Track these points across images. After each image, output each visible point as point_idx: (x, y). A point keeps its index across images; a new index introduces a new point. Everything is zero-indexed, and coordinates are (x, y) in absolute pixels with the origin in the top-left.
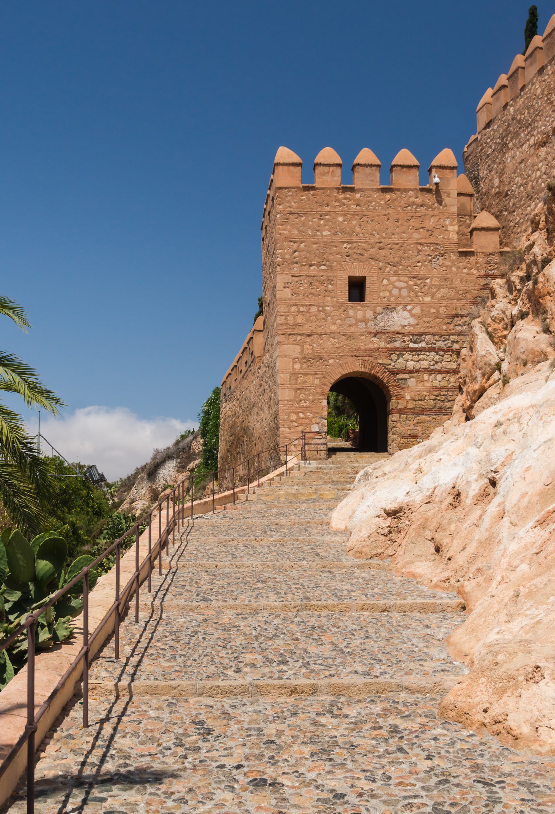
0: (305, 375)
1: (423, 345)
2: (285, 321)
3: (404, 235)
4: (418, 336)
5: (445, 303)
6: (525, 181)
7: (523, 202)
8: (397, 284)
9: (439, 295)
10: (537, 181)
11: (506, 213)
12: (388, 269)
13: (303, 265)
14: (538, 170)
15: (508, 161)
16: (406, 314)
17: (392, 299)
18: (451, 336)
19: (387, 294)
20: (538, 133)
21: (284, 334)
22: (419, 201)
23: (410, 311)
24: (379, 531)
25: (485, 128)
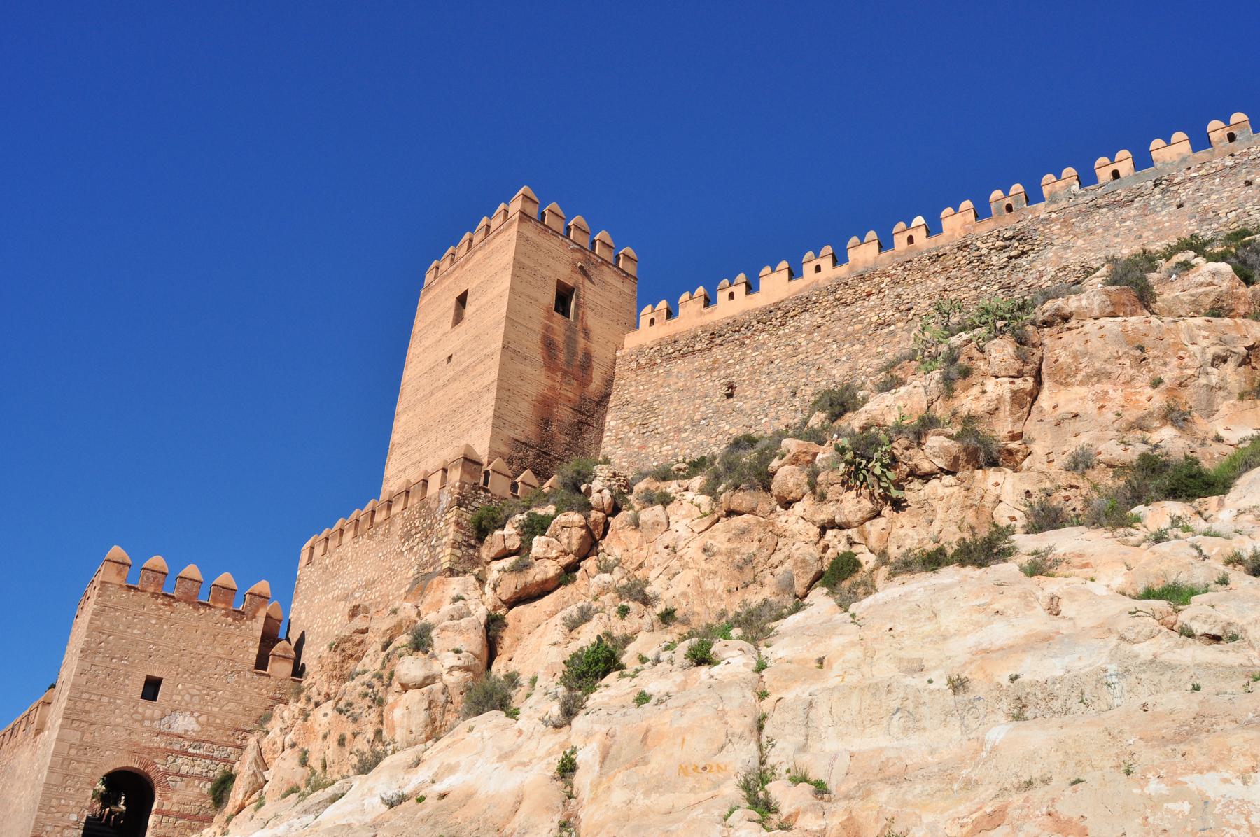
0: (78, 762)
4: (198, 742)
5: (231, 716)
16: (193, 720)
19: (179, 698)
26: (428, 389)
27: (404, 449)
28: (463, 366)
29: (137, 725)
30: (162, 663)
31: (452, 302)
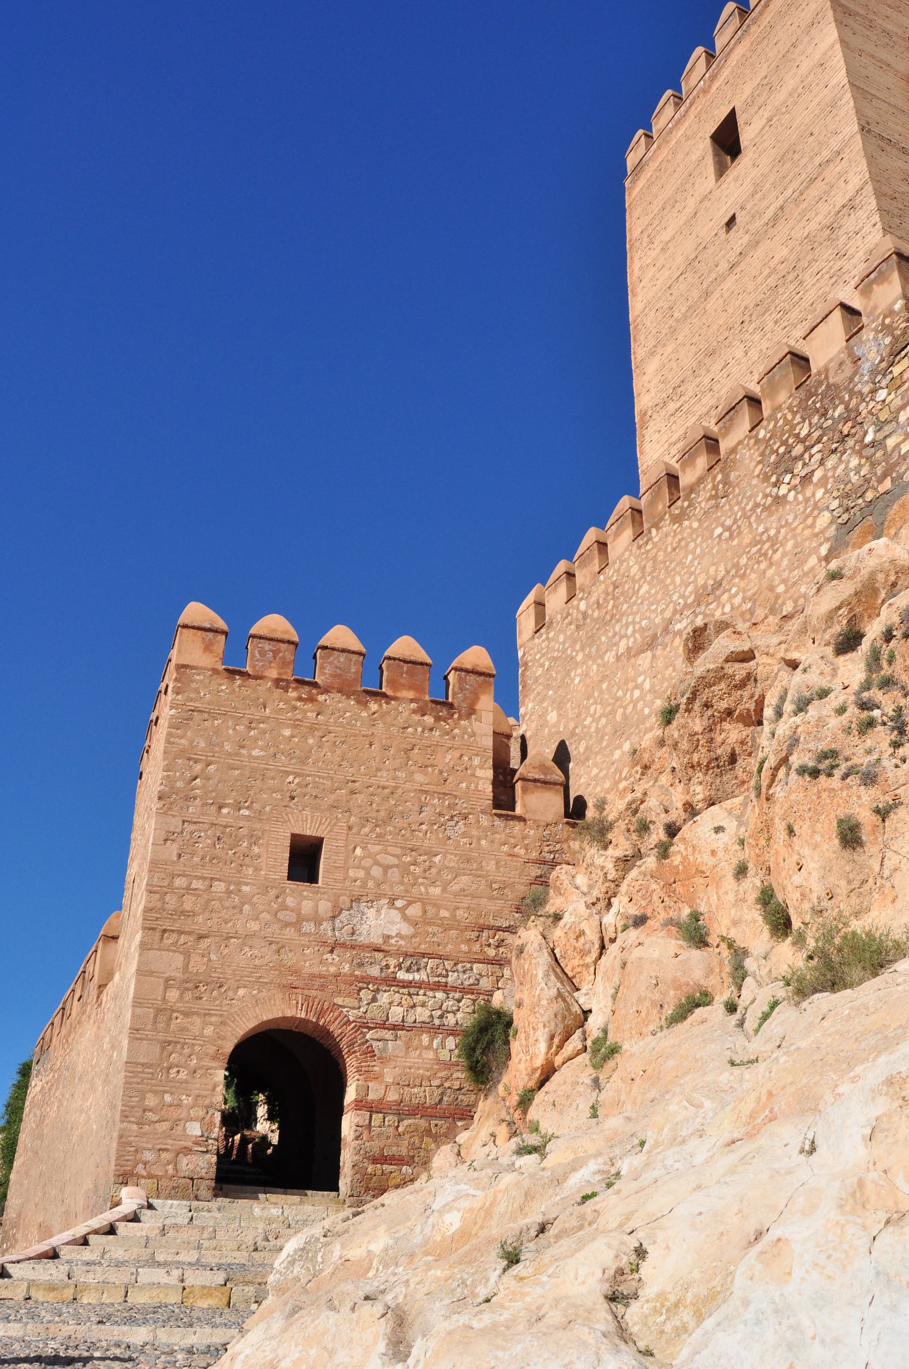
2: (159, 904)
3: (399, 774)
5: (466, 902)
6: (609, 709)
7: (604, 744)
9: (455, 887)
10: (635, 706)
12: (367, 830)
13: (206, 804)
14: (637, 687)
15: (577, 681)
16: (395, 915)
18: (475, 966)
20: (634, 631)
21: (152, 929)
23: (402, 910)
25: (533, 638)
26: (695, 294)
27: (672, 406)
28: (770, 213)
29: (290, 932)
30: (316, 808)
31: (705, 146)
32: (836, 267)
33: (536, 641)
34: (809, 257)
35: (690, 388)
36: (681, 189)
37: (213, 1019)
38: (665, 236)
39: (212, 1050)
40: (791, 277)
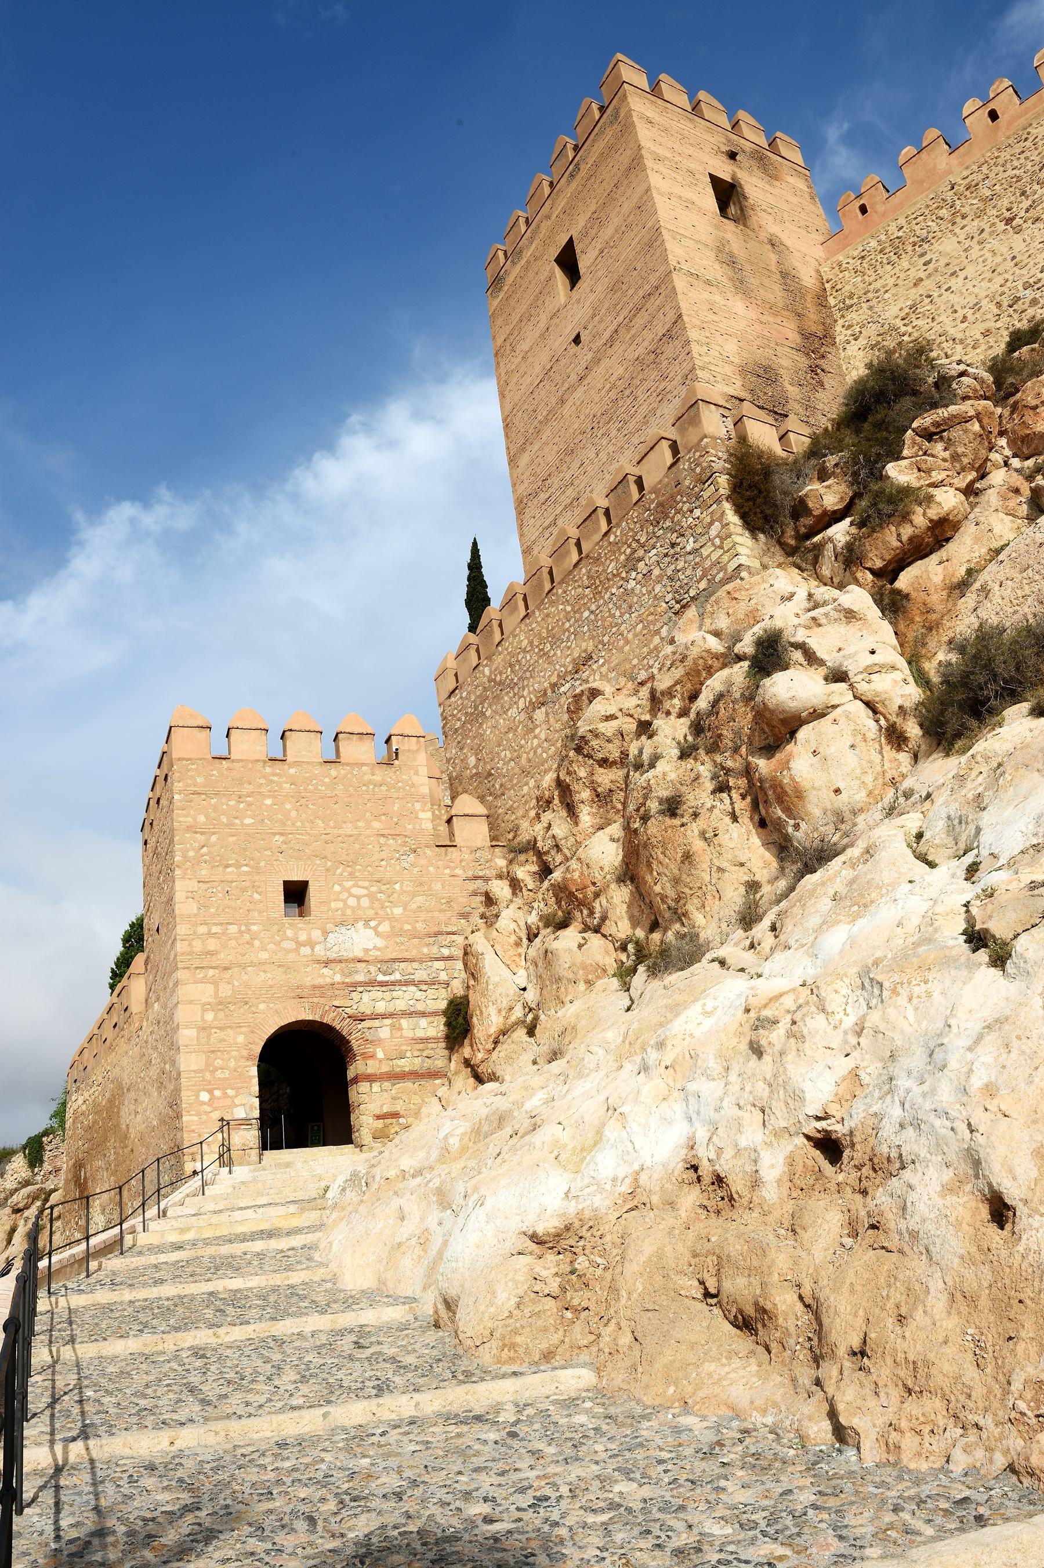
1: (396, 976)
4: (388, 963)
5: (423, 916)
8: (354, 891)
9: (414, 906)
11: (490, 798)
12: (339, 871)
14: (535, 737)
16: (370, 933)
17: (349, 912)
19: (341, 905)
22: (377, 778)
23: (375, 929)
24: (537, 1288)
26: (554, 400)
27: (543, 496)
28: (607, 334)
29: (291, 957)
30: (299, 859)
32: (661, 387)
33: (453, 699)
34: (640, 377)
35: (555, 482)
36: (534, 305)
37: (243, 1030)
38: (525, 346)
39: (245, 1053)
40: (627, 392)
